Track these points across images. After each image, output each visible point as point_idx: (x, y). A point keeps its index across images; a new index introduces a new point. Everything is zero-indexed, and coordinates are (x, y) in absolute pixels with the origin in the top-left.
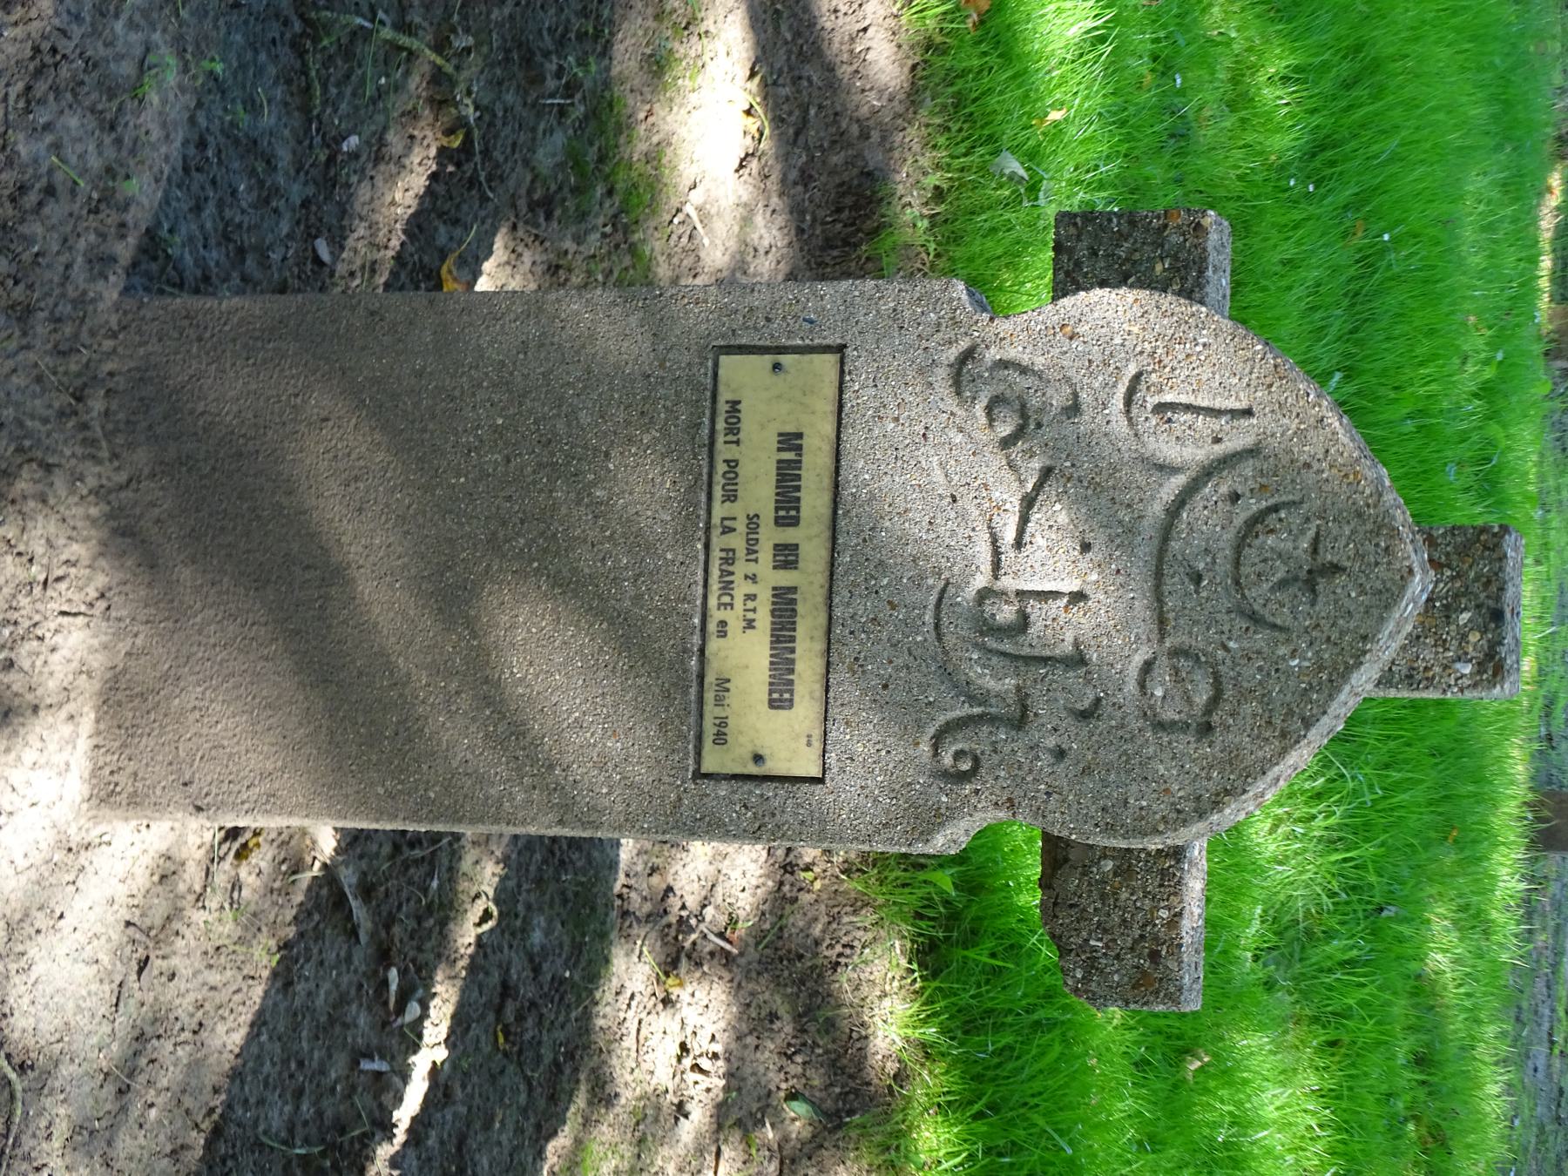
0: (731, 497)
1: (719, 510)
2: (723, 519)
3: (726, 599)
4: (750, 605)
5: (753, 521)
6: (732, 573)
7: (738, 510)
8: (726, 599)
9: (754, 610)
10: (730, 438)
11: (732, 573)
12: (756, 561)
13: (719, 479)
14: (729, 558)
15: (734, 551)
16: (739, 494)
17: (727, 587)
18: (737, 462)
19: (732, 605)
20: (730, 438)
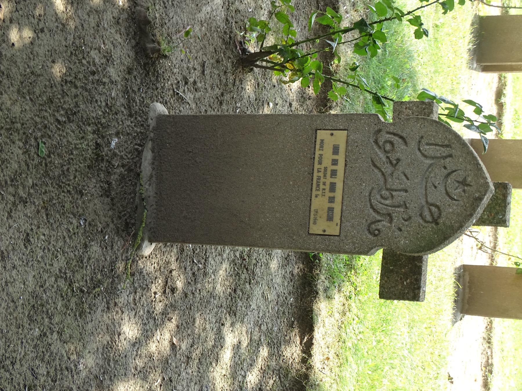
0: (320, 163)
1: (317, 166)
2: (318, 169)
3: (318, 188)
4: (324, 191)
5: (326, 169)
6: (320, 182)
7: (322, 167)
8: (318, 188)
9: (325, 193)
10: (321, 149)
11: (320, 182)
12: (326, 178)
13: (317, 159)
14: (319, 178)
15: (320, 176)
17: (318, 186)
18: (322, 155)
20: (321, 149)
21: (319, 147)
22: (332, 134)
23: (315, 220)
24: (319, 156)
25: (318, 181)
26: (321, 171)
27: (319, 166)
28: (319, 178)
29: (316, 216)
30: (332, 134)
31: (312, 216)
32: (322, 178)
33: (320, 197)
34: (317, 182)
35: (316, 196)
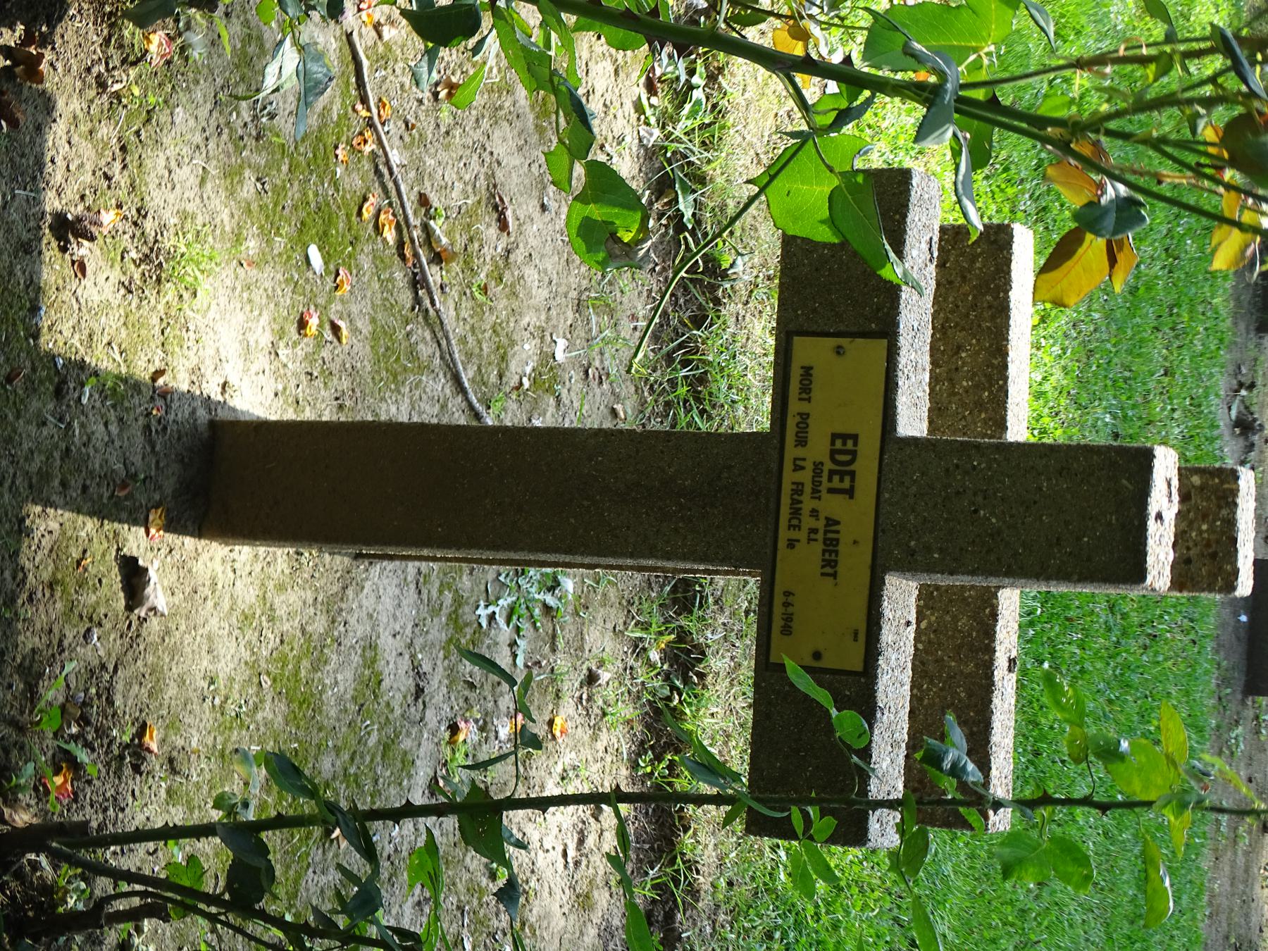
0: (802, 441)
1: (791, 451)
2: (795, 459)
3: (795, 522)
6: (801, 502)
8: (795, 522)
11: (801, 502)
14: (798, 489)
15: (803, 484)
17: (796, 512)
18: (808, 415)
19: (799, 527)
20: (804, 396)
21: (797, 391)
22: (839, 351)
23: (786, 620)
24: (798, 419)
25: (795, 497)
26: (802, 468)
27: (800, 452)
28: (798, 489)
29: (790, 609)
30: (839, 351)
31: (778, 610)
32: (808, 489)
33: (802, 547)
34: (795, 502)
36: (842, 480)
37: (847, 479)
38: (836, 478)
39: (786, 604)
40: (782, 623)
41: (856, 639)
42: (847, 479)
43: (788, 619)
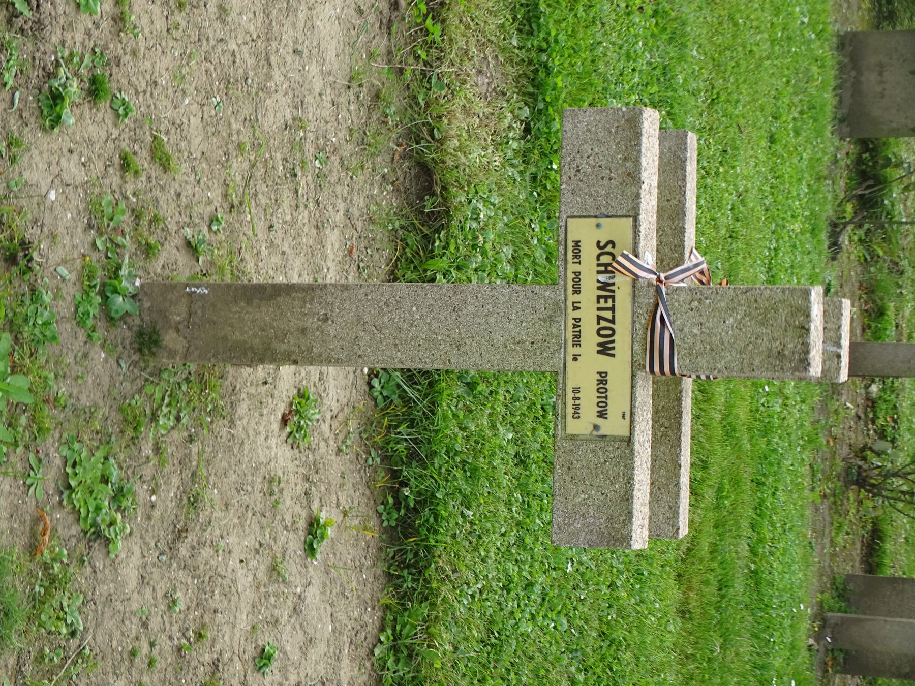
0: (577, 291)
1: (572, 298)
2: (574, 303)
16: (582, 290)
17: (577, 337)
20: (576, 260)
26: (579, 308)
27: (576, 298)
29: (577, 402)
31: (570, 402)
35: (575, 359)
36: (606, 302)
37: (610, 300)
38: (602, 301)
39: (575, 399)
40: (573, 411)
41: (624, 417)
42: (610, 300)
43: (577, 408)
